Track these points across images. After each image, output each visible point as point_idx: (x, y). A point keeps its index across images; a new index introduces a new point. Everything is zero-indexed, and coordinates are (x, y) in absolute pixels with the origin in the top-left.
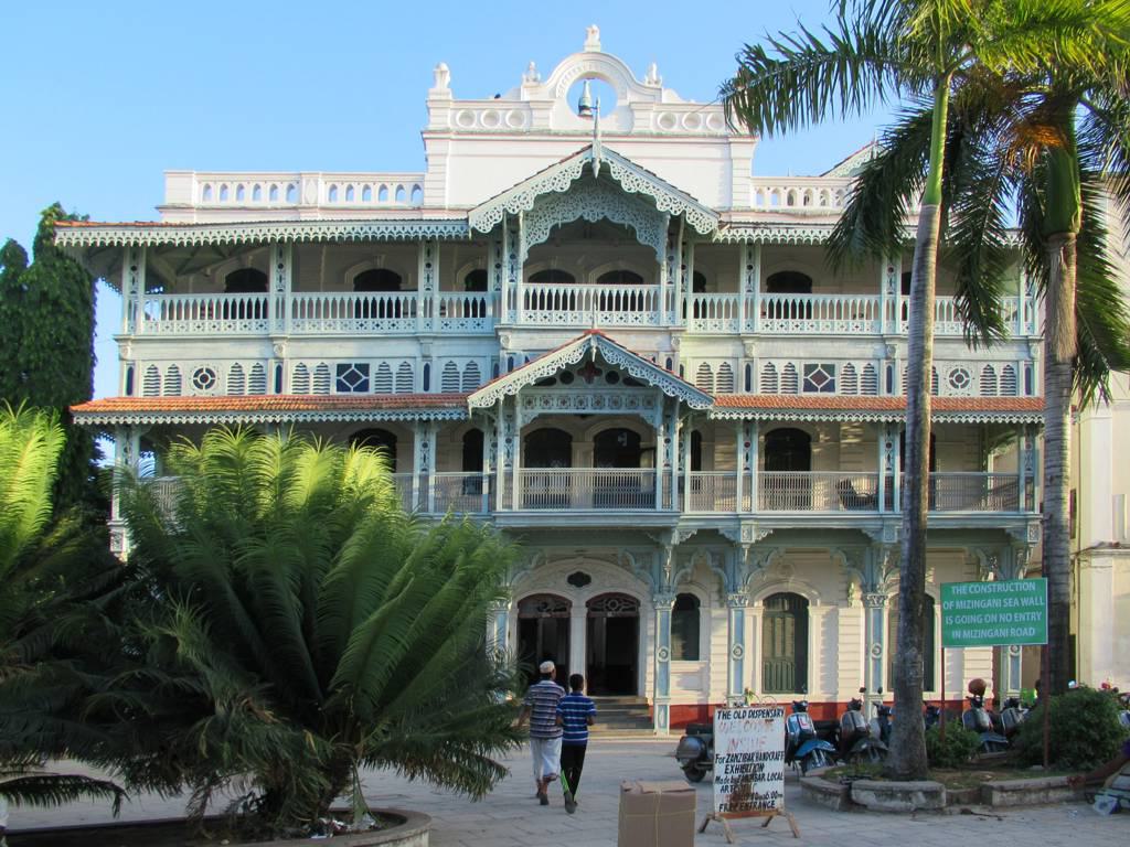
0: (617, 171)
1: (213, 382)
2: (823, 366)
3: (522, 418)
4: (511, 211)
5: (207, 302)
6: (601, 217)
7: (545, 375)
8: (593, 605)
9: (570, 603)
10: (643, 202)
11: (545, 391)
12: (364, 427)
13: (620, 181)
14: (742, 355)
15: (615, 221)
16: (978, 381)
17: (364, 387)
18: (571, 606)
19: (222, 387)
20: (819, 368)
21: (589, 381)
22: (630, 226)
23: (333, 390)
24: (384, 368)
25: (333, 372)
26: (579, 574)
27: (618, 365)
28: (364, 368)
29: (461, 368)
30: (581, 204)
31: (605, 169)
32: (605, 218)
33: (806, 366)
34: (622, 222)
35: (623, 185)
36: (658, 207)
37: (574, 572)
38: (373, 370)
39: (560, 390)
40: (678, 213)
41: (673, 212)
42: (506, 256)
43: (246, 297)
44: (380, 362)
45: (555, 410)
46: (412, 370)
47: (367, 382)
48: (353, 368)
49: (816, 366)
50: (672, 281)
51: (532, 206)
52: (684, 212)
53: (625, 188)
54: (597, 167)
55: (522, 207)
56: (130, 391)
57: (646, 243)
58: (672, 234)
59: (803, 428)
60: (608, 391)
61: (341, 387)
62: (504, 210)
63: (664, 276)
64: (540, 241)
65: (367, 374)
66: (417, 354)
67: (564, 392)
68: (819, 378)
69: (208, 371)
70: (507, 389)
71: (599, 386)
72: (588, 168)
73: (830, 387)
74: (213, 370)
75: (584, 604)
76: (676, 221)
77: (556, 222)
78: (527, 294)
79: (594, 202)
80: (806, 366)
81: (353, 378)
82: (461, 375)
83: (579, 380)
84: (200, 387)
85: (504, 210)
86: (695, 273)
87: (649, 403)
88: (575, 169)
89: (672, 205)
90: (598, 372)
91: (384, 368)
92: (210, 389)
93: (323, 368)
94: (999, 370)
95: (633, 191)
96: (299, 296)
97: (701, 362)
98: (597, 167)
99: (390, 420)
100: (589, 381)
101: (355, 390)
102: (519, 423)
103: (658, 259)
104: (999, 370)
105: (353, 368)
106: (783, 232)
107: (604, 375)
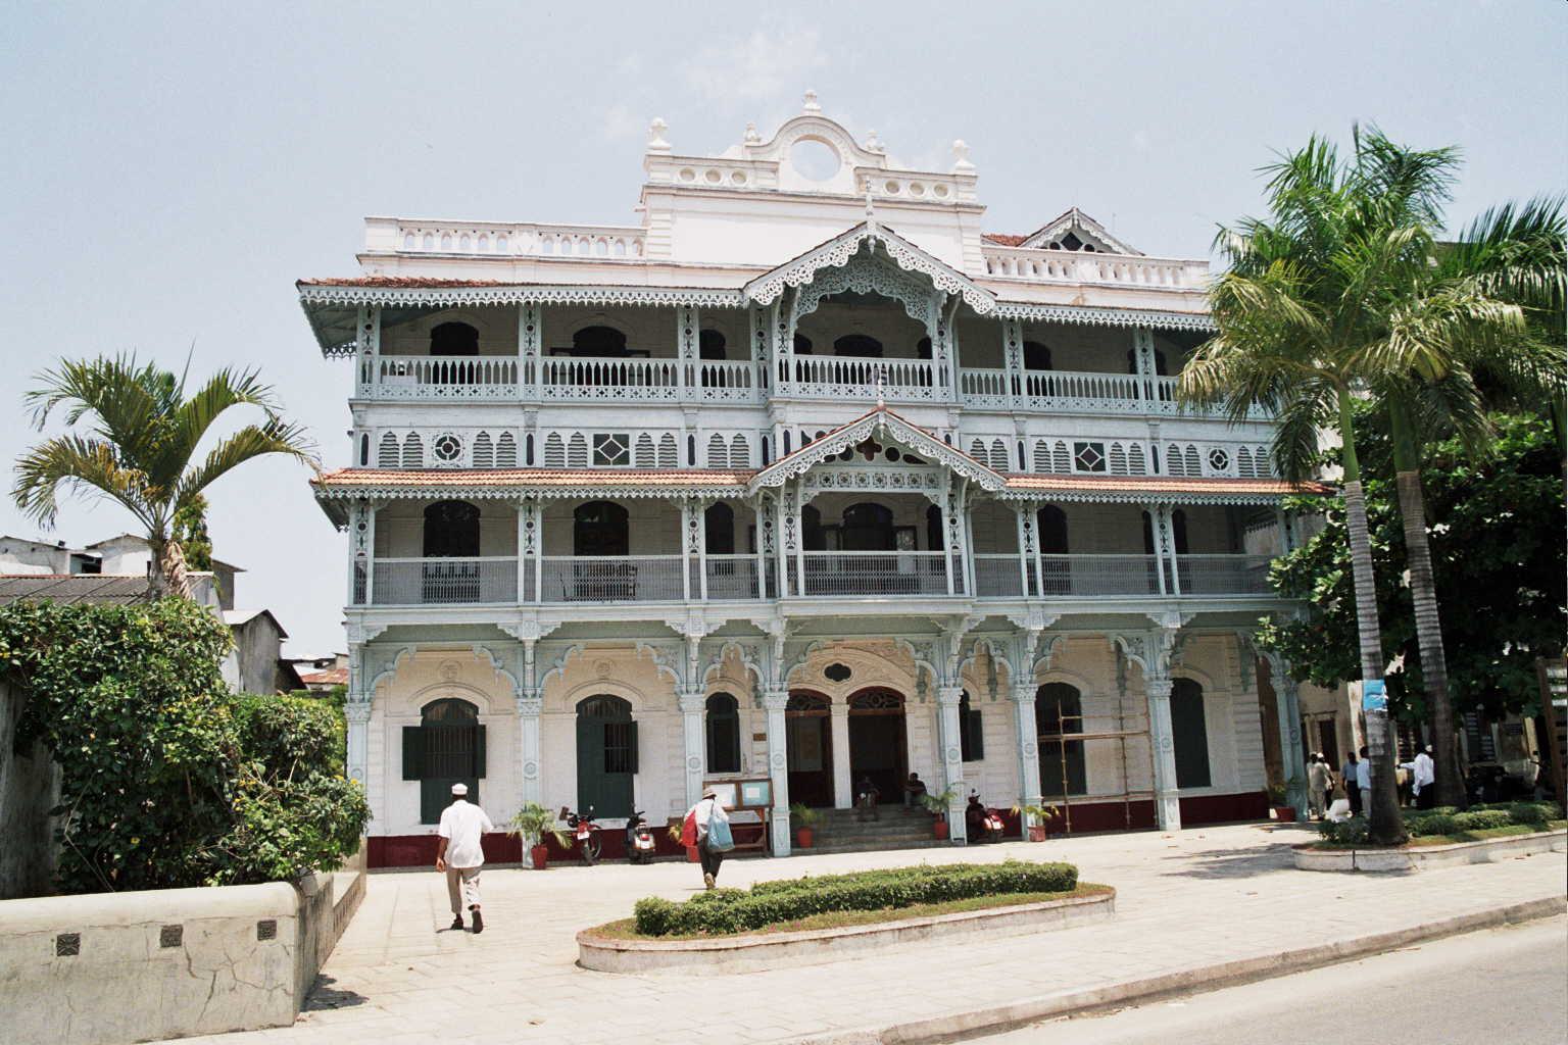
0: (893, 249)
1: (457, 452)
3: (805, 495)
4: (790, 284)
5: (501, 364)
6: (869, 289)
8: (855, 700)
10: (921, 284)
13: (896, 259)
15: (883, 294)
18: (831, 703)
21: (871, 458)
23: (590, 463)
24: (645, 439)
25: (590, 441)
26: (838, 666)
30: (848, 277)
31: (880, 245)
32: (873, 290)
33: (1076, 444)
36: (936, 285)
38: (633, 441)
40: (955, 292)
41: (950, 291)
44: (640, 433)
45: (836, 488)
46: (676, 442)
47: (627, 454)
50: (945, 354)
51: (811, 280)
52: (961, 291)
53: (902, 266)
55: (801, 280)
56: (364, 461)
58: (946, 309)
60: (889, 470)
61: (598, 459)
65: (626, 445)
66: (682, 425)
67: (845, 470)
69: (452, 439)
72: (863, 244)
74: (458, 438)
75: (844, 700)
78: (799, 364)
79: (860, 274)
80: (1076, 444)
82: (728, 448)
84: (444, 457)
85: (785, 283)
88: (852, 247)
89: (948, 284)
90: (879, 449)
91: (645, 439)
92: (455, 460)
93: (578, 437)
95: (909, 269)
99: (629, 497)
100: (871, 458)
102: (801, 503)
107: (884, 450)
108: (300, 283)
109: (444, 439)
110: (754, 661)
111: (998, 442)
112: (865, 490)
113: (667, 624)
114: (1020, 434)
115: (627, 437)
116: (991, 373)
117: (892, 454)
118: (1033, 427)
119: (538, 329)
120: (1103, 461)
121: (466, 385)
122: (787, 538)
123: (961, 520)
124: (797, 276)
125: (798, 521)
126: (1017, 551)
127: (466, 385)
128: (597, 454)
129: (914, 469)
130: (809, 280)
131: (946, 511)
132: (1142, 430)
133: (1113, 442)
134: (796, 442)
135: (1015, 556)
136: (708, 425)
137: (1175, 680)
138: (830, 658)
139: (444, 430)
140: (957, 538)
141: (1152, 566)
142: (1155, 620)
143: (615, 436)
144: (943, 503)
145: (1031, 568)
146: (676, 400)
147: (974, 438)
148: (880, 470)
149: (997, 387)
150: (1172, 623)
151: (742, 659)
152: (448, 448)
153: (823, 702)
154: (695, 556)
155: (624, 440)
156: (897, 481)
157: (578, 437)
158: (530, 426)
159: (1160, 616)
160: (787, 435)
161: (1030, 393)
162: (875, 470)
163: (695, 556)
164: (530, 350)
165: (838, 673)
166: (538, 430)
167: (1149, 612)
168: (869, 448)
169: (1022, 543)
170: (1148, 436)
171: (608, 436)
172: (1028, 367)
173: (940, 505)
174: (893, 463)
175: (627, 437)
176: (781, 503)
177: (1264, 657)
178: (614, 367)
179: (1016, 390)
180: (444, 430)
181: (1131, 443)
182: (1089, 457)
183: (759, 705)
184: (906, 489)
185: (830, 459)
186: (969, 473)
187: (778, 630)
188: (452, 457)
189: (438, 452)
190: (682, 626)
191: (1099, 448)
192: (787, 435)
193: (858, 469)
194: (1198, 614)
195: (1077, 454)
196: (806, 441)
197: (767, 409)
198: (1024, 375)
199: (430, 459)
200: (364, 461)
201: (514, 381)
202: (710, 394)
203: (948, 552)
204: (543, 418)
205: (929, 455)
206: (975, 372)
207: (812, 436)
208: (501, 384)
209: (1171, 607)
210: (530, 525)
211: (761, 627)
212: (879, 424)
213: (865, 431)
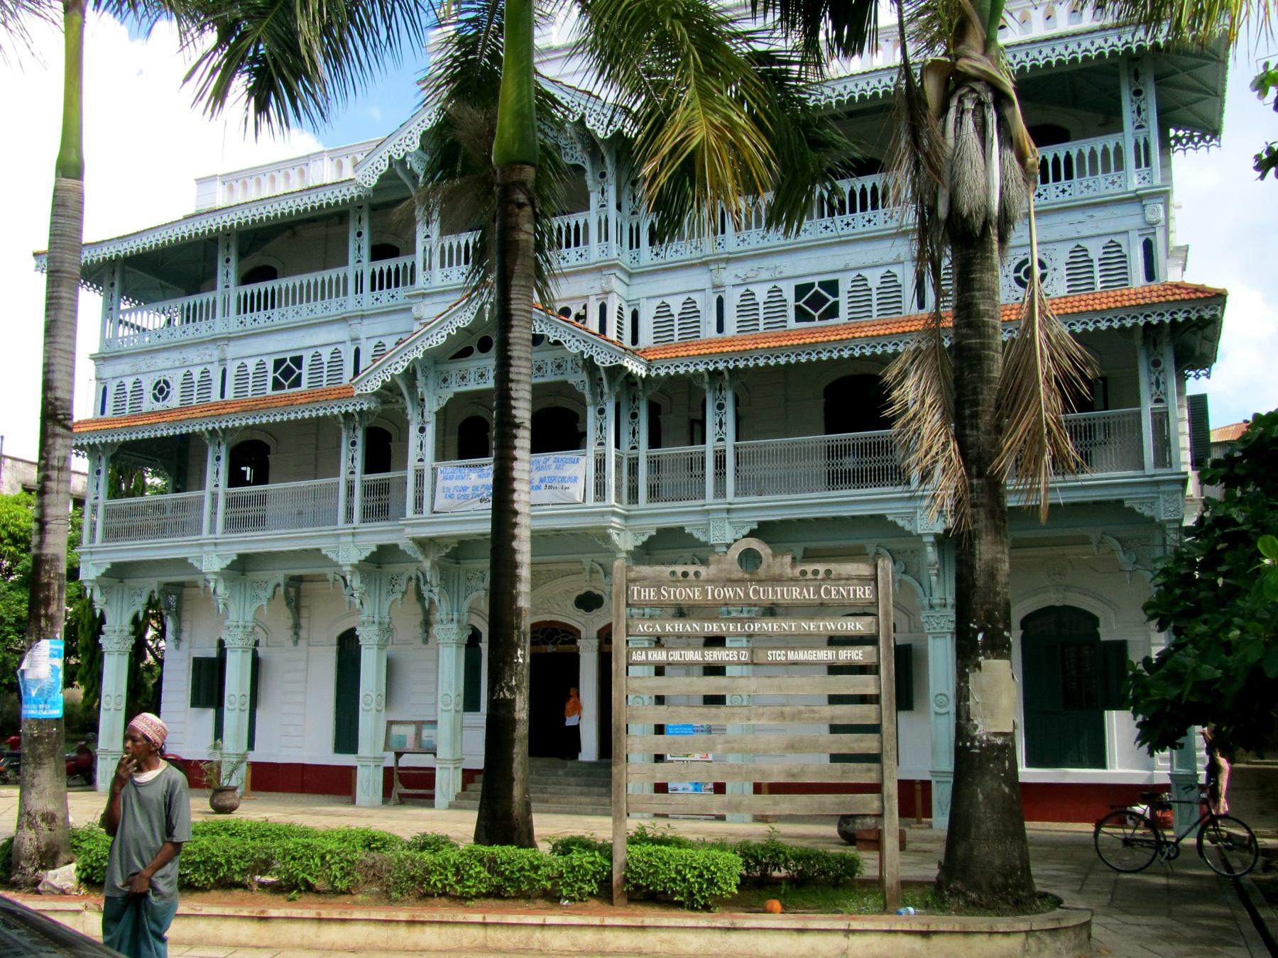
2: (821, 284)
7: (434, 345)
9: (579, 632)
14: (709, 285)
16: (1063, 271)
19: (174, 401)
20: (816, 287)
23: (269, 391)
25: (270, 367)
37: (582, 592)
49: (812, 285)
56: (103, 412)
61: (277, 385)
62: (391, 157)
63: (594, 199)
67: (481, 363)
68: (817, 301)
73: (833, 312)
75: (595, 634)
94: (1095, 251)
97: (658, 302)
102: (432, 406)
104: (1095, 251)
108: (35, 255)
111: (690, 301)
114: (716, 287)
124: (404, 146)
133: (853, 275)
142: (900, 523)
145: (350, 489)
153: (570, 635)
154: (351, 477)
156: (559, 366)
158: (222, 360)
159: (911, 517)
163: (351, 477)
167: (891, 511)
180: (158, 374)
183: (426, 641)
200: (103, 412)
213: (468, 314)
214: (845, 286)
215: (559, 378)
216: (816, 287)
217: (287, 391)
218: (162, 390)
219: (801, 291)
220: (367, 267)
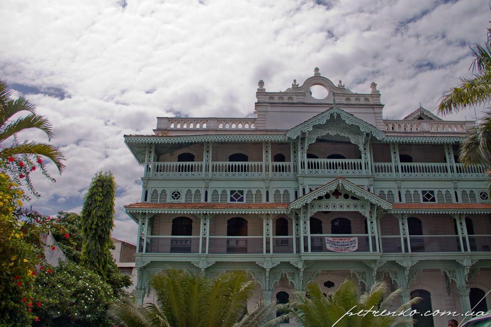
1: (179, 197)
3: (311, 212)
6: (336, 133)
11: (320, 202)
12: (234, 217)
17: (242, 200)
20: (428, 192)
21: (337, 198)
22: (348, 137)
23: (229, 201)
24: (250, 192)
25: (229, 193)
27: (351, 191)
28: (242, 192)
29: (282, 192)
31: (339, 116)
34: (344, 135)
35: (346, 121)
39: (325, 202)
42: (299, 148)
43: (187, 163)
47: (242, 198)
48: (237, 192)
50: (367, 157)
54: (335, 115)
56: (146, 200)
57: (355, 143)
59: (416, 217)
60: (345, 202)
61: (232, 200)
64: (313, 142)
65: (242, 194)
66: (264, 187)
69: (178, 192)
70: (306, 201)
71: (341, 200)
72: (332, 115)
76: (367, 135)
77: (318, 135)
81: (237, 196)
83: (333, 197)
86: (400, 156)
87: (362, 207)
90: (340, 194)
91: (250, 192)
93: (224, 192)
96: (215, 163)
98: (335, 115)
100: (337, 198)
101: (238, 201)
102: (309, 215)
103: (360, 149)
105: (237, 192)
106: (409, 139)
107: (343, 195)
109: (175, 192)
110: (294, 279)
111: (390, 191)
112: (343, 210)
113: (257, 263)
115: (243, 191)
116: (386, 164)
117: (346, 196)
118: (405, 185)
119: (211, 152)
120: (434, 197)
121: (184, 172)
122: (303, 229)
123: (375, 222)
124: (306, 128)
125: (308, 223)
126: (399, 234)
127: (184, 172)
128: (231, 198)
129: (355, 202)
130: (311, 129)
131: (368, 218)
132: (451, 185)
134: (307, 191)
135: (262, 237)
136: (274, 186)
137: (471, 289)
138: (326, 279)
139: (174, 189)
140: (374, 229)
141: (458, 239)
142: (460, 262)
143: (238, 191)
144: (367, 215)
146: (262, 177)
147: (380, 190)
148: (341, 202)
149: (389, 170)
150: (467, 263)
151: (288, 277)
152: (176, 195)
154: (268, 236)
155: (242, 192)
157: (224, 192)
159: (462, 261)
160: (304, 190)
161: (402, 172)
162: (339, 202)
164: (207, 160)
165: (329, 284)
166: (209, 189)
167: (457, 259)
168: (337, 193)
169: (401, 231)
170: (453, 187)
171: (236, 191)
172: (401, 161)
173: (366, 216)
174: (347, 200)
175: (243, 191)
176: (301, 215)
177: (452, 280)
178: (223, 165)
179: (397, 171)
180: (174, 189)
181: (446, 190)
182: (428, 196)
184: (352, 210)
185: (320, 198)
186: (377, 202)
187: (300, 266)
188: (177, 199)
189: (172, 197)
190: (263, 264)
191: (432, 192)
192: (304, 190)
193: (332, 202)
194: (479, 260)
195: (231, 195)
196: (311, 190)
197: (297, 180)
198: (400, 164)
199: (169, 200)
200: (146, 200)
201: (201, 171)
202: (214, 175)
203: (370, 235)
204: (213, 185)
205: (360, 195)
206: (380, 164)
207: (312, 189)
208: (190, 172)
209: (466, 257)
210: (205, 224)
211: (294, 265)
212: (339, 184)
214: (436, 193)
215: (356, 210)
216: (428, 192)
217: (237, 202)
218: (176, 195)
219: (424, 192)
220: (272, 164)
